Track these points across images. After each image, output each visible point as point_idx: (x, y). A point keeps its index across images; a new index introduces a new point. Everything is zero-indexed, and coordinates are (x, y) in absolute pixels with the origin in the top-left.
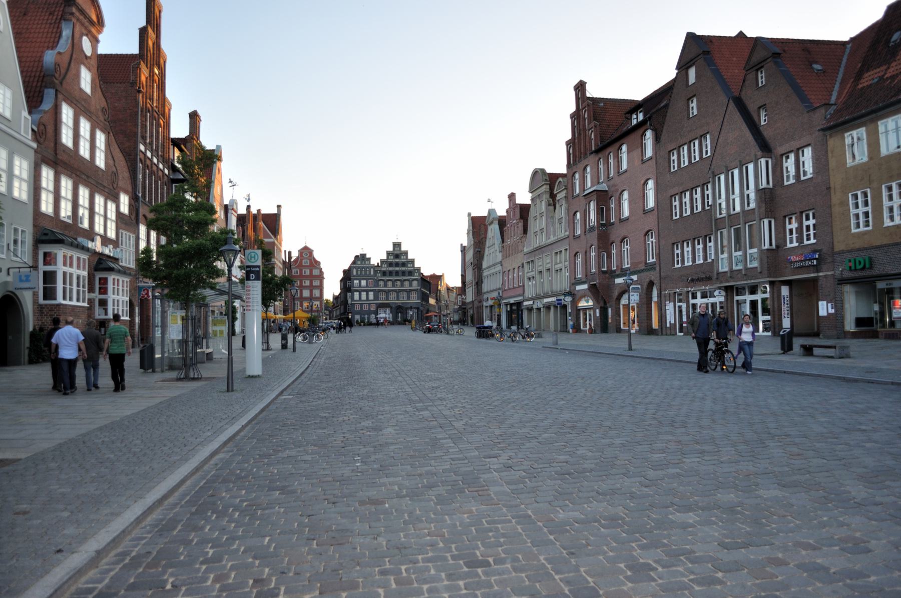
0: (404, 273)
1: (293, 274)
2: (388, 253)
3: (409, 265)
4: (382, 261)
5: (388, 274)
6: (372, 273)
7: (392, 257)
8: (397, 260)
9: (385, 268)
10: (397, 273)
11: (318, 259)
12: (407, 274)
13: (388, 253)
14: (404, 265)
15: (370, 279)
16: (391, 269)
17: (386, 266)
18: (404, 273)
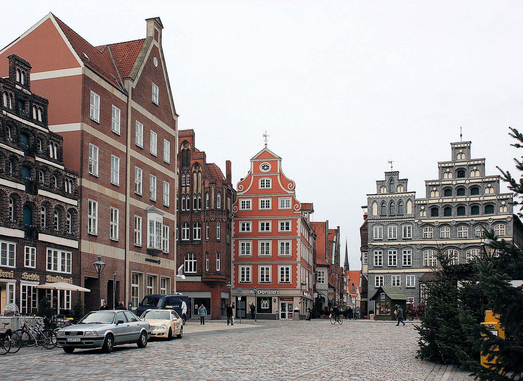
0: (475, 209)
1: (241, 209)
2: (443, 168)
3: (487, 191)
4: (430, 186)
5: (441, 211)
6: (410, 211)
7: (450, 176)
8: (461, 181)
9: (436, 198)
10: (461, 209)
11: (288, 175)
12: (482, 209)
13: (443, 168)
14: (475, 190)
15: (407, 223)
16: (447, 200)
17: (437, 194)
18: (475, 209)
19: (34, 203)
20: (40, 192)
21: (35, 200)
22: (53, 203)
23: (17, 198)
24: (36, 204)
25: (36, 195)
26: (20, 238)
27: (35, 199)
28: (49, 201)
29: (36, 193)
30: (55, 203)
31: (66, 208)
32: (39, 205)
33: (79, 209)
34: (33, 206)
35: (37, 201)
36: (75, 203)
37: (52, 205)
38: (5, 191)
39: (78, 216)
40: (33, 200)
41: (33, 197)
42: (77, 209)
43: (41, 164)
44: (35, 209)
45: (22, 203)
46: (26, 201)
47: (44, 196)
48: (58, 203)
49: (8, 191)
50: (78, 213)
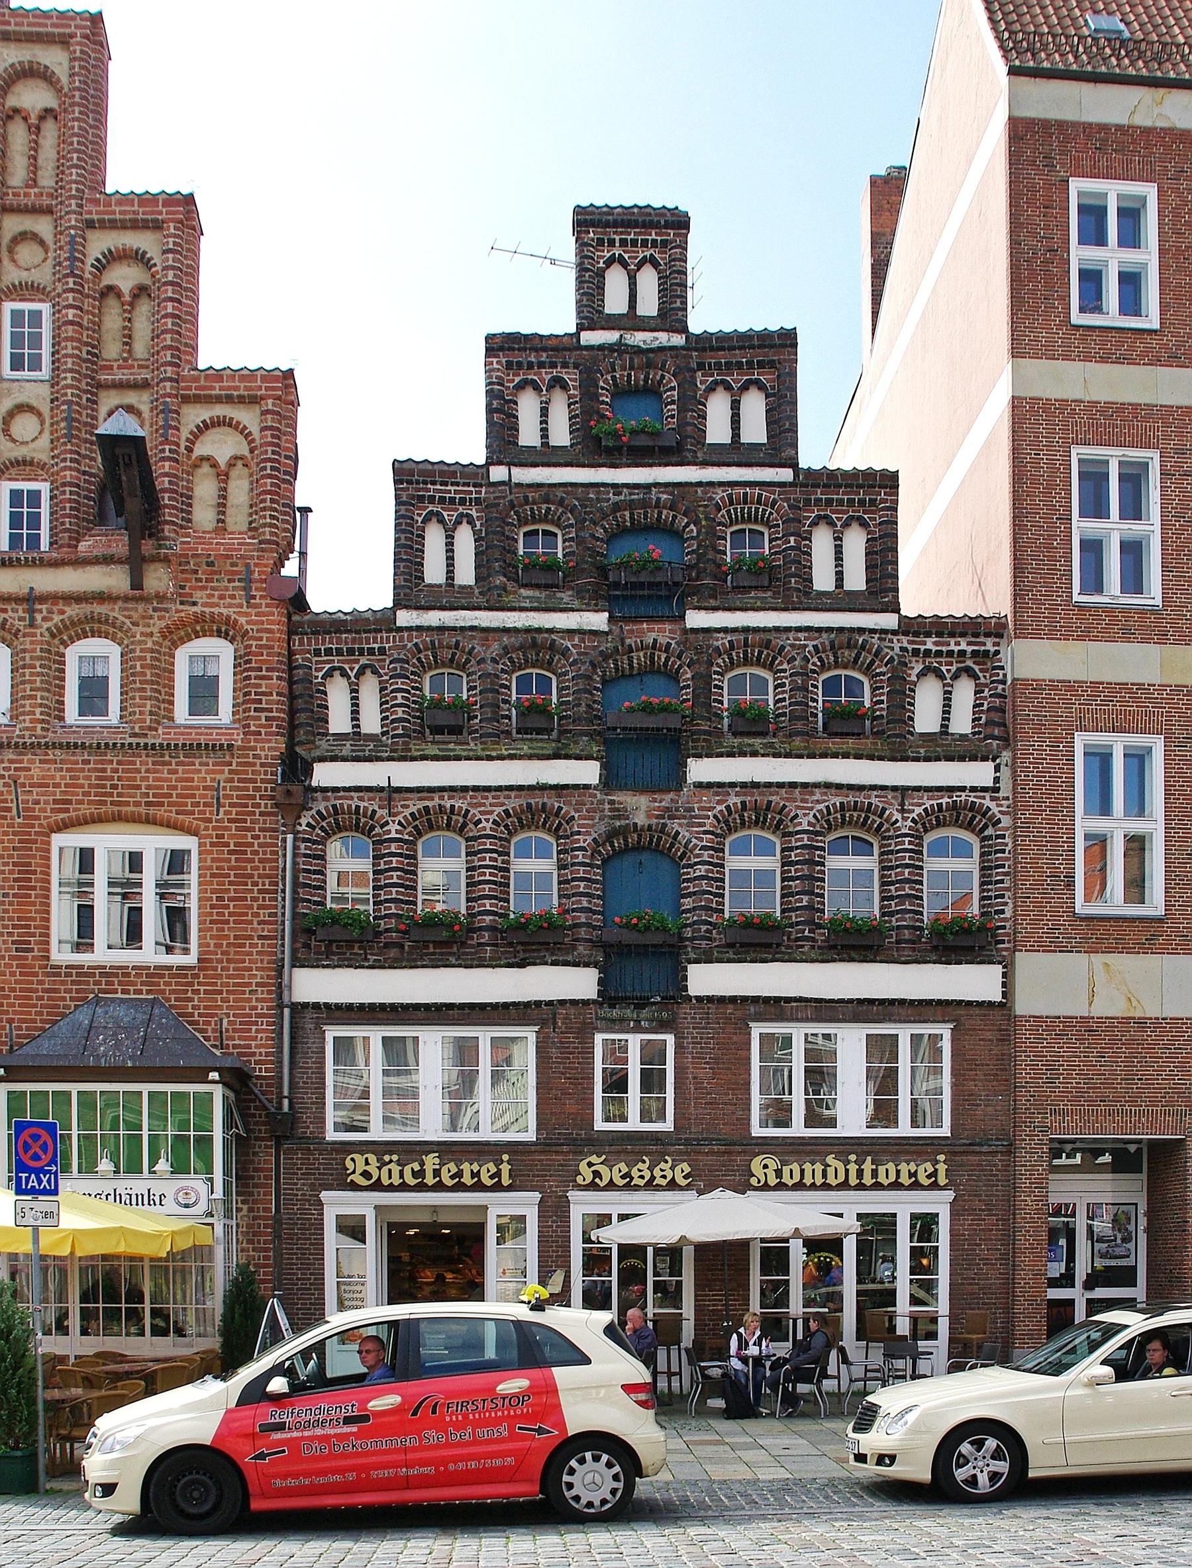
19: (663, 829)
20: (701, 770)
21: (670, 813)
22: (798, 807)
23: (560, 824)
24: (677, 833)
25: (679, 788)
26: (574, 1002)
27: (668, 809)
28: (770, 802)
29: (677, 779)
30: (818, 802)
31: (902, 811)
32: (697, 832)
33: (1007, 799)
34: (672, 845)
35: (684, 817)
36: (979, 773)
37: (796, 816)
38: (467, 811)
39: (1003, 837)
40: (658, 817)
41: (655, 801)
42: (992, 805)
43: (722, 641)
44: (684, 853)
45: (578, 841)
46: (602, 828)
47: (732, 785)
48: (837, 800)
49: (484, 805)
50: (999, 821)
